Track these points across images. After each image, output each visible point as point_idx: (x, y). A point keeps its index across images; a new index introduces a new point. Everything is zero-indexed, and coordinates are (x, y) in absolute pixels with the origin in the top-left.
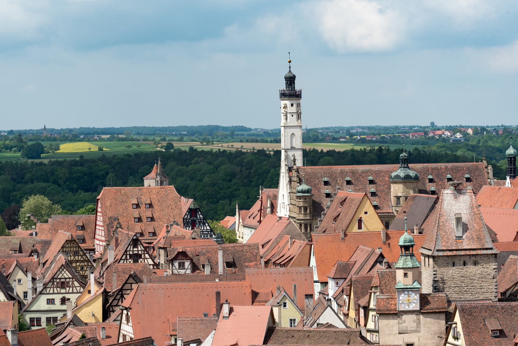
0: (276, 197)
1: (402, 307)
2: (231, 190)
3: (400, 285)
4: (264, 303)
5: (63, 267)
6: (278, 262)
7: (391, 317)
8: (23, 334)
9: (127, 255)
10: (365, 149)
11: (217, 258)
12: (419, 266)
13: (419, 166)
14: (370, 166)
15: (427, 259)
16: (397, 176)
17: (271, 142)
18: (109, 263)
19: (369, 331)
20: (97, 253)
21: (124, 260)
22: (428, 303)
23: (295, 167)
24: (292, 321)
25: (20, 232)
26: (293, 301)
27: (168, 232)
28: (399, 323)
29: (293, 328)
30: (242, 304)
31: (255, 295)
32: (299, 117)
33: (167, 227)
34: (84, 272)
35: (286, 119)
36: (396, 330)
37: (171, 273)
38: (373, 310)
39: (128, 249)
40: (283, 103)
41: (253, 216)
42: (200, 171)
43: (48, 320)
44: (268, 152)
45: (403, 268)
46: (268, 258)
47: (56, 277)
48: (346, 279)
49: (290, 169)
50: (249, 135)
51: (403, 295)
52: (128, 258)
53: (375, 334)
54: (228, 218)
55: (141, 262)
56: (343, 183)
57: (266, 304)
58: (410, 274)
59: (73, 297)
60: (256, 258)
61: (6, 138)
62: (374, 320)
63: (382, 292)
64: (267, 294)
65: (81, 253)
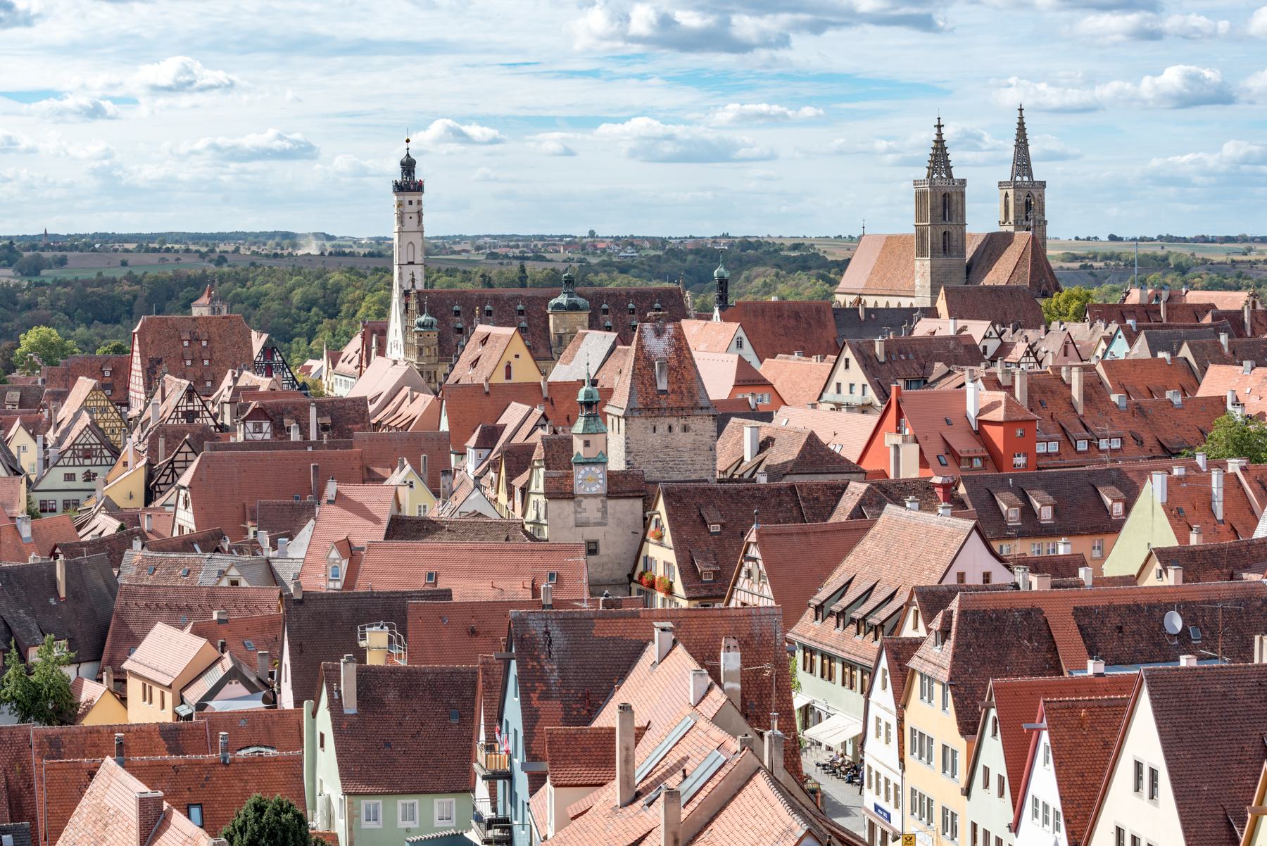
6: (393, 424)
28: (576, 512)
36: (571, 521)
49: (406, 294)
63: (548, 467)
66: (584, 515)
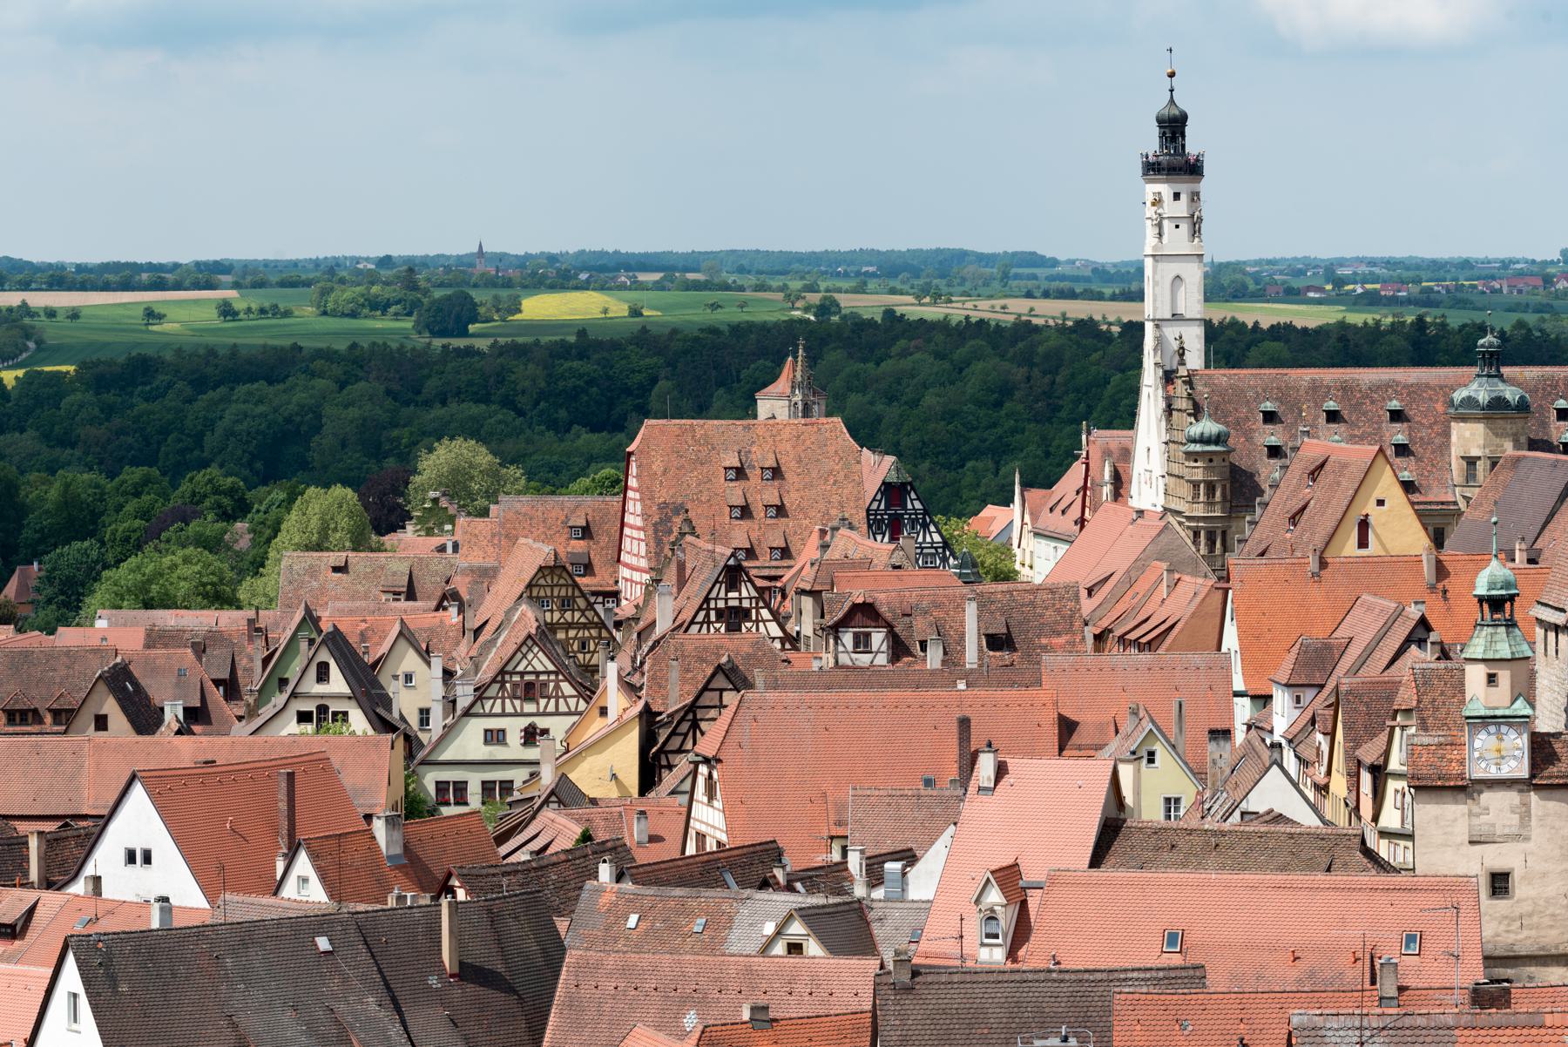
0: (1126, 454)
1: (1479, 771)
2: (999, 431)
3: (1476, 708)
4: (1091, 753)
5: (530, 643)
6: (1132, 636)
7: (1448, 795)
8: (419, 827)
9: (708, 609)
10: (1378, 323)
11: (963, 621)
12: (1529, 654)
13: (1531, 373)
14: (1393, 370)
15: (1551, 635)
16: (1470, 402)
17: (1114, 298)
18: (658, 631)
19: (1384, 834)
20: (624, 602)
21: (702, 624)
22: (1552, 758)
23: (1183, 372)
24: (1171, 803)
25: (410, 542)
26: (1174, 747)
27: (825, 547)
28: (1470, 814)
29: (1173, 823)
30: (1032, 753)
31: (1067, 728)
32: (1195, 231)
33: (823, 532)
34: (588, 656)
35: (1160, 235)
36: (1461, 832)
37: (831, 664)
38: (1398, 776)
39: (713, 595)
40: (1152, 189)
41: (1062, 505)
42: (913, 377)
43: (487, 787)
44: (1104, 327)
45: (1484, 660)
46: (1105, 623)
47: (509, 668)
48: (1322, 686)
49: (1169, 377)
50: (1051, 278)
51: (1483, 735)
52: (713, 618)
53: (1402, 843)
54: (990, 511)
55: (749, 630)
56: (1316, 417)
57: (1099, 754)
58: (1504, 676)
59: (558, 726)
60: (1072, 625)
61: (372, 278)
62: (1399, 805)
63: (1423, 726)
64: (1101, 727)
65: (581, 603)
66: (1484, 818)
